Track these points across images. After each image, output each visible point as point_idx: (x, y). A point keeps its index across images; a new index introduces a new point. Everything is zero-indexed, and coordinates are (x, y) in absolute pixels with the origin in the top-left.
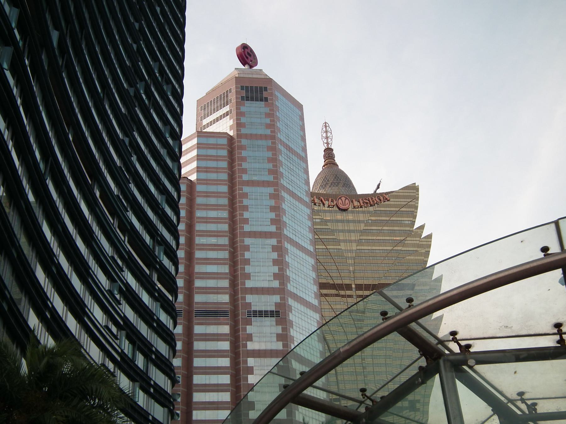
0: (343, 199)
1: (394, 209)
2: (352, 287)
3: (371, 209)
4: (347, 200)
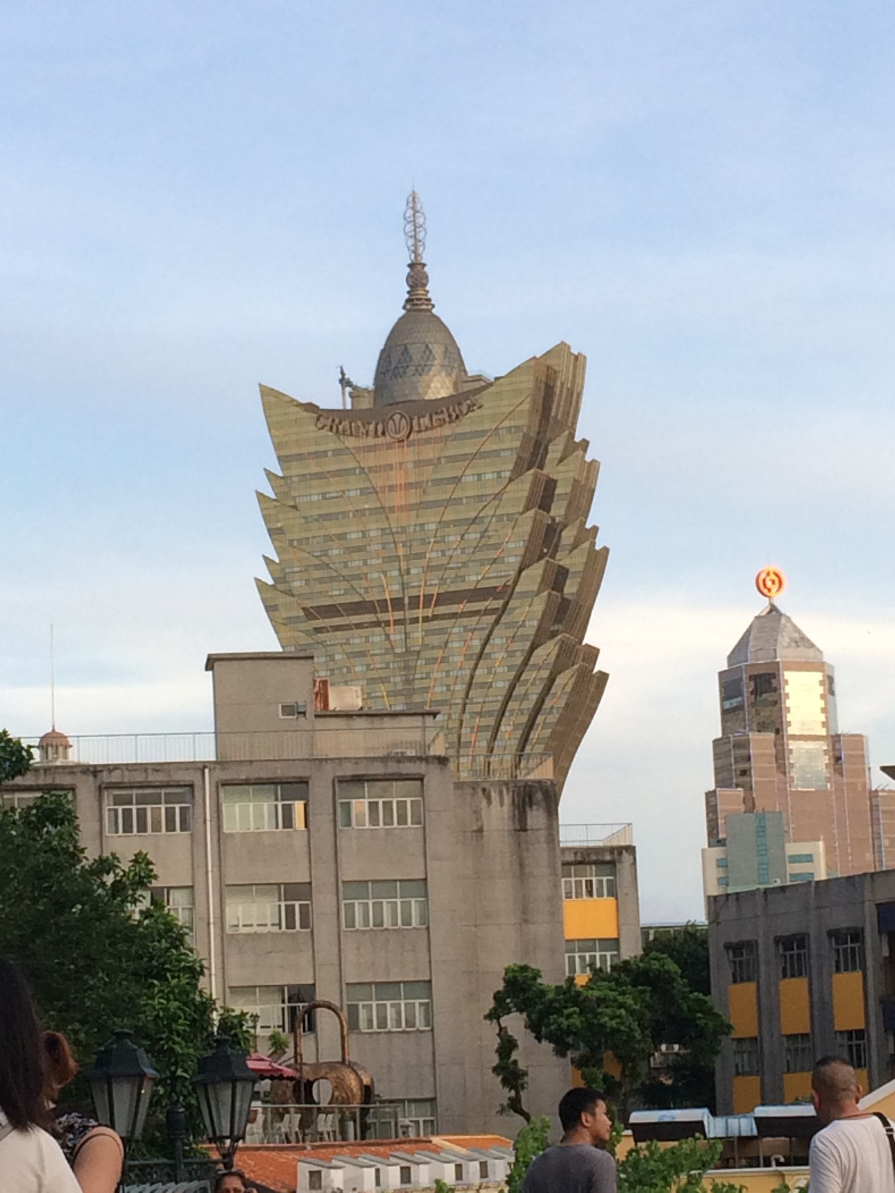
0: (397, 417)
1: (486, 426)
2: (403, 605)
3: (447, 430)
4: (403, 420)
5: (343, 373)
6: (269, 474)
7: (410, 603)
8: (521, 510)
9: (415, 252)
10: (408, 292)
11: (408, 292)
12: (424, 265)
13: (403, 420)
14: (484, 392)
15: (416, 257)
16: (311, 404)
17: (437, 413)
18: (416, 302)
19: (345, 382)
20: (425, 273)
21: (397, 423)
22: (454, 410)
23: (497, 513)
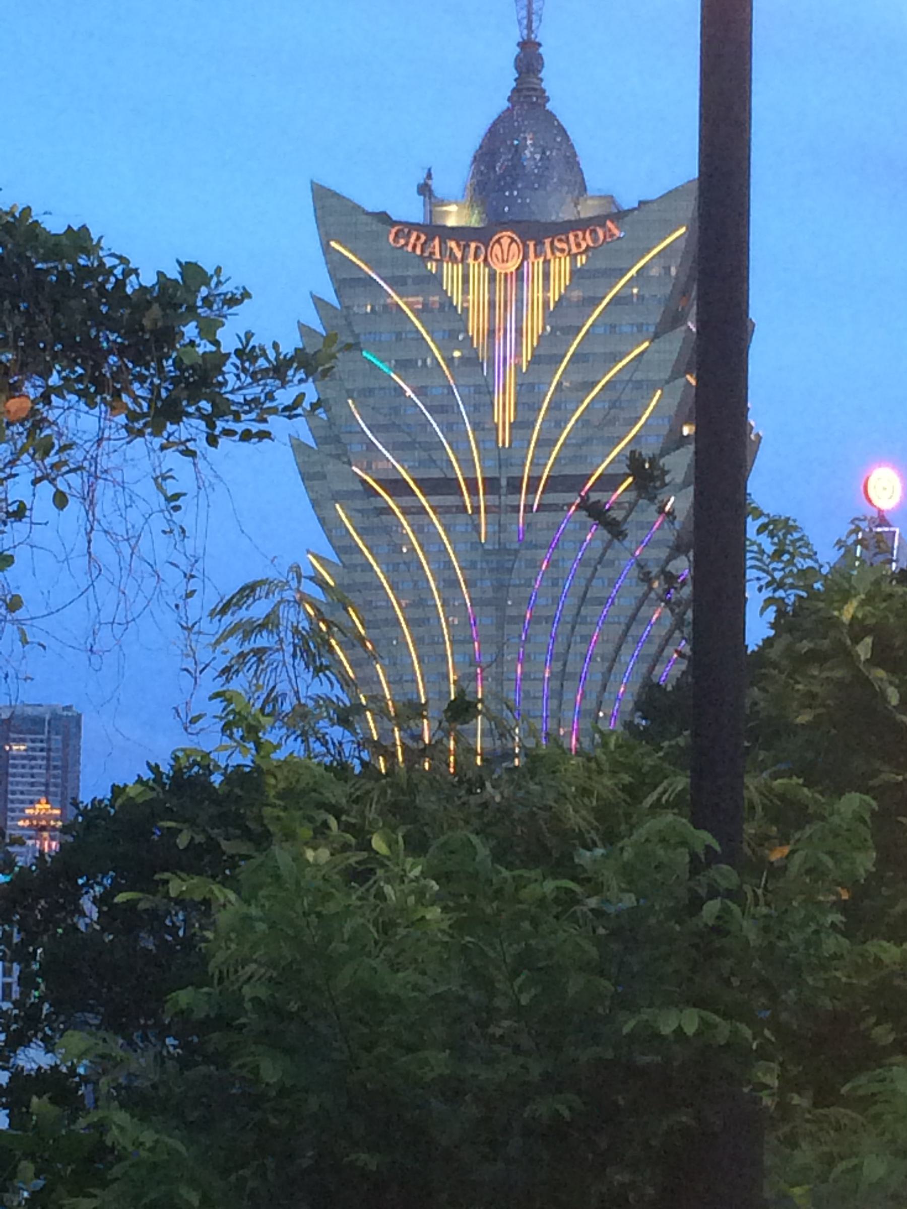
0: (505, 241)
2: (500, 487)
4: (514, 246)
5: (429, 176)
6: (319, 303)
7: (508, 484)
8: (667, 377)
9: (529, 27)
10: (516, 80)
11: (516, 80)
12: (540, 45)
13: (514, 246)
14: (627, 219)
15: (528, 35)
16: (384, 214)
17: (560, 240)
18: (525, 93)
19: (425, 189)
20: (540, 56)
21: (505, 248)
22: (584, 239)
23: (634, 379)
